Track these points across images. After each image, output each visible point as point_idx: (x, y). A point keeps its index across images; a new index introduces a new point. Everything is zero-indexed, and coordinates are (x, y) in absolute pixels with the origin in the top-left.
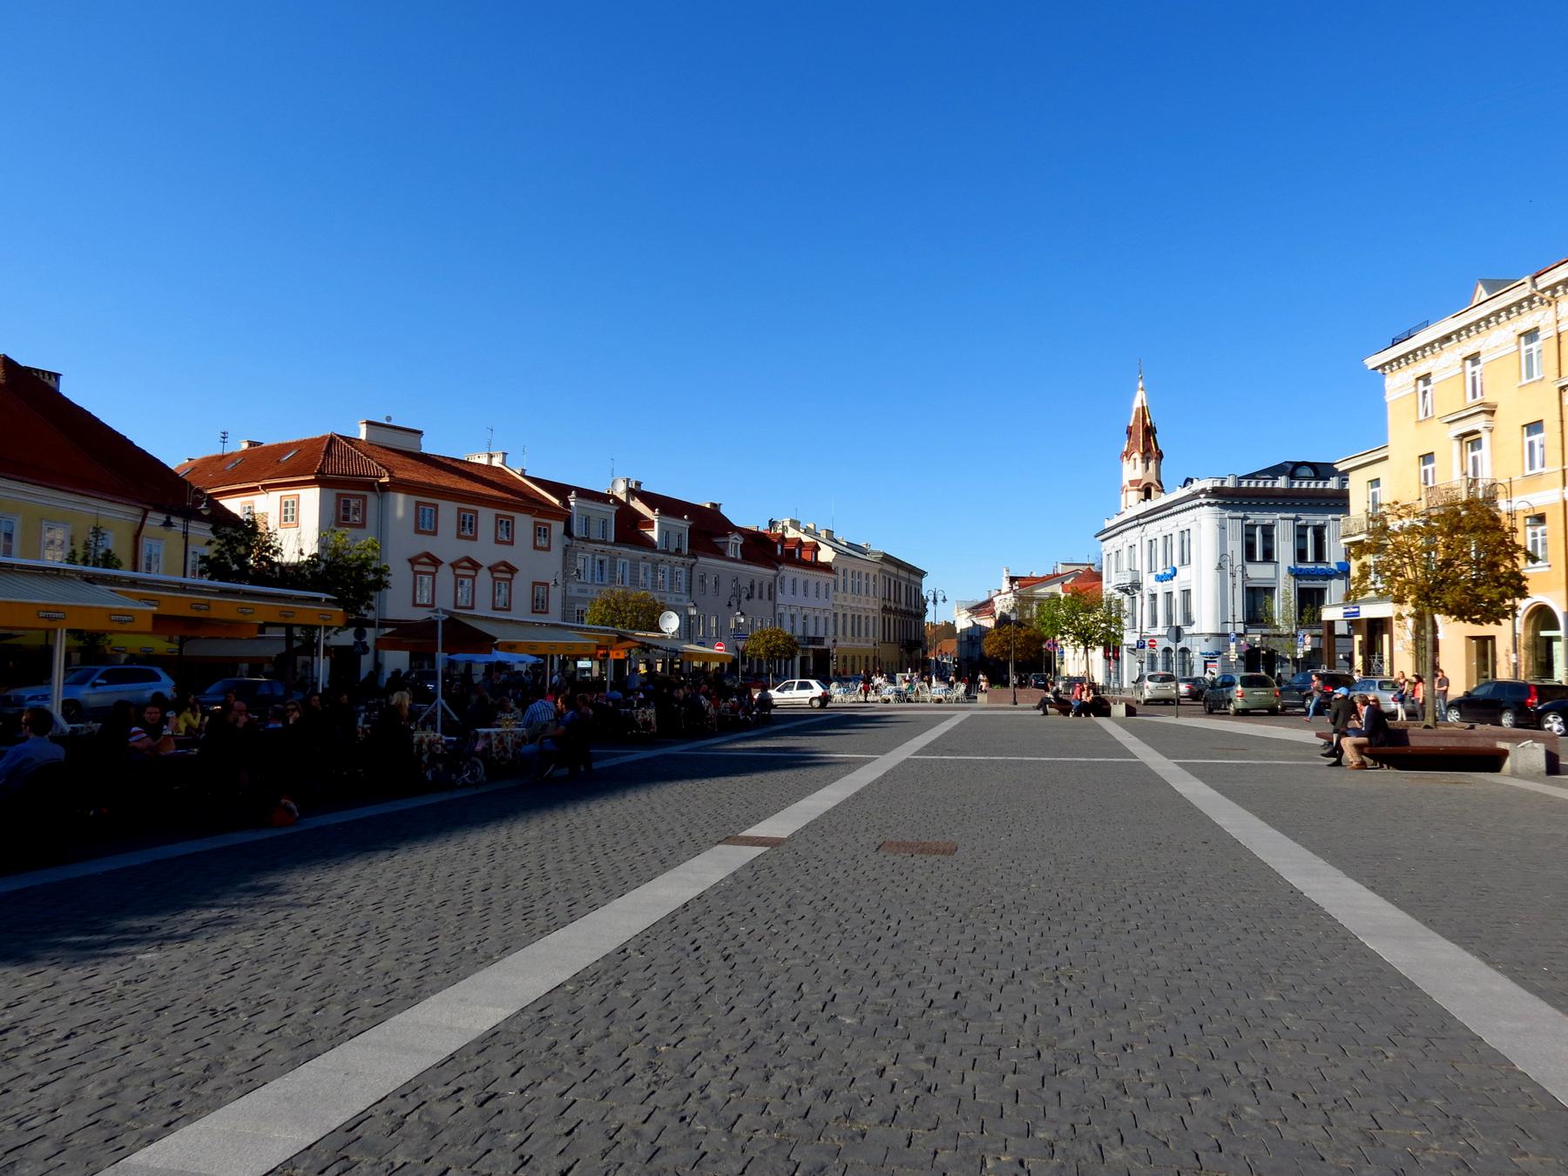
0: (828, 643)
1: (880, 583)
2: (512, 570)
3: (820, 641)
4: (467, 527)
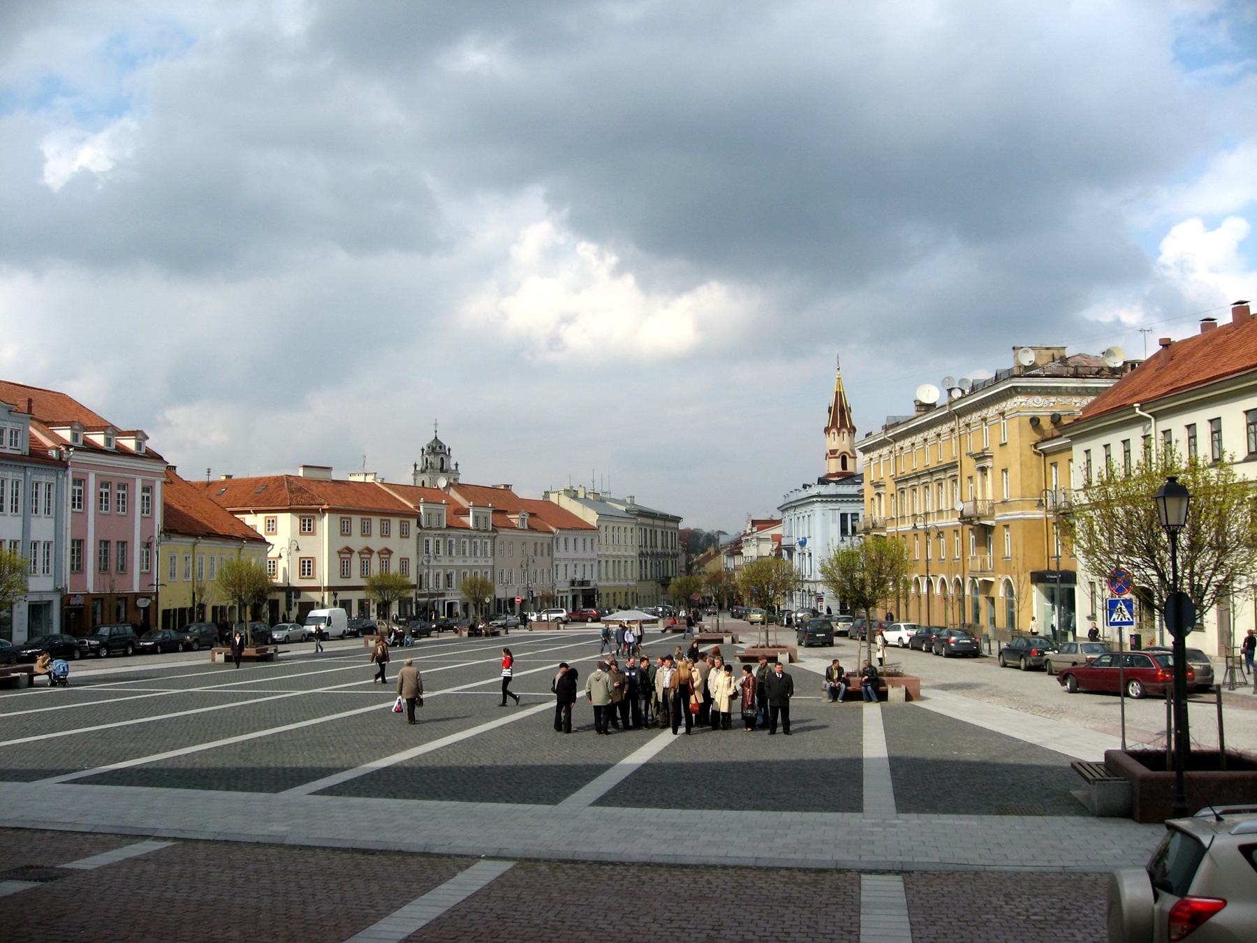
0: (592, 585)
1: (637, 533)
2: (389, 552)
3: (587, 583)
4: (366, 532)
